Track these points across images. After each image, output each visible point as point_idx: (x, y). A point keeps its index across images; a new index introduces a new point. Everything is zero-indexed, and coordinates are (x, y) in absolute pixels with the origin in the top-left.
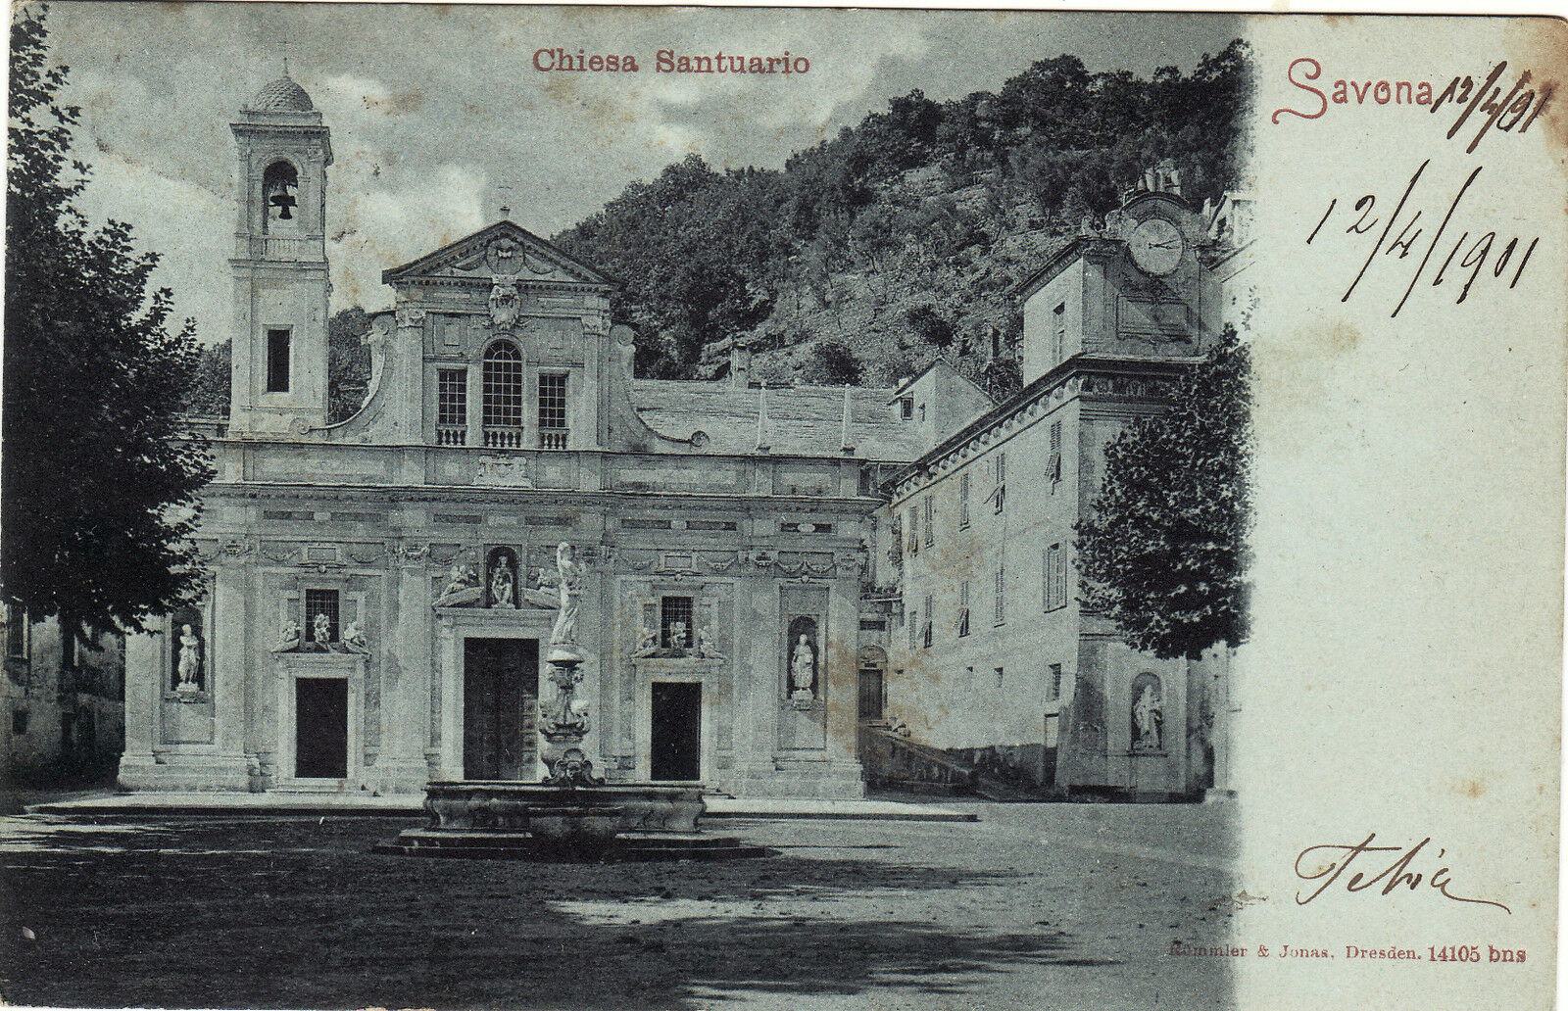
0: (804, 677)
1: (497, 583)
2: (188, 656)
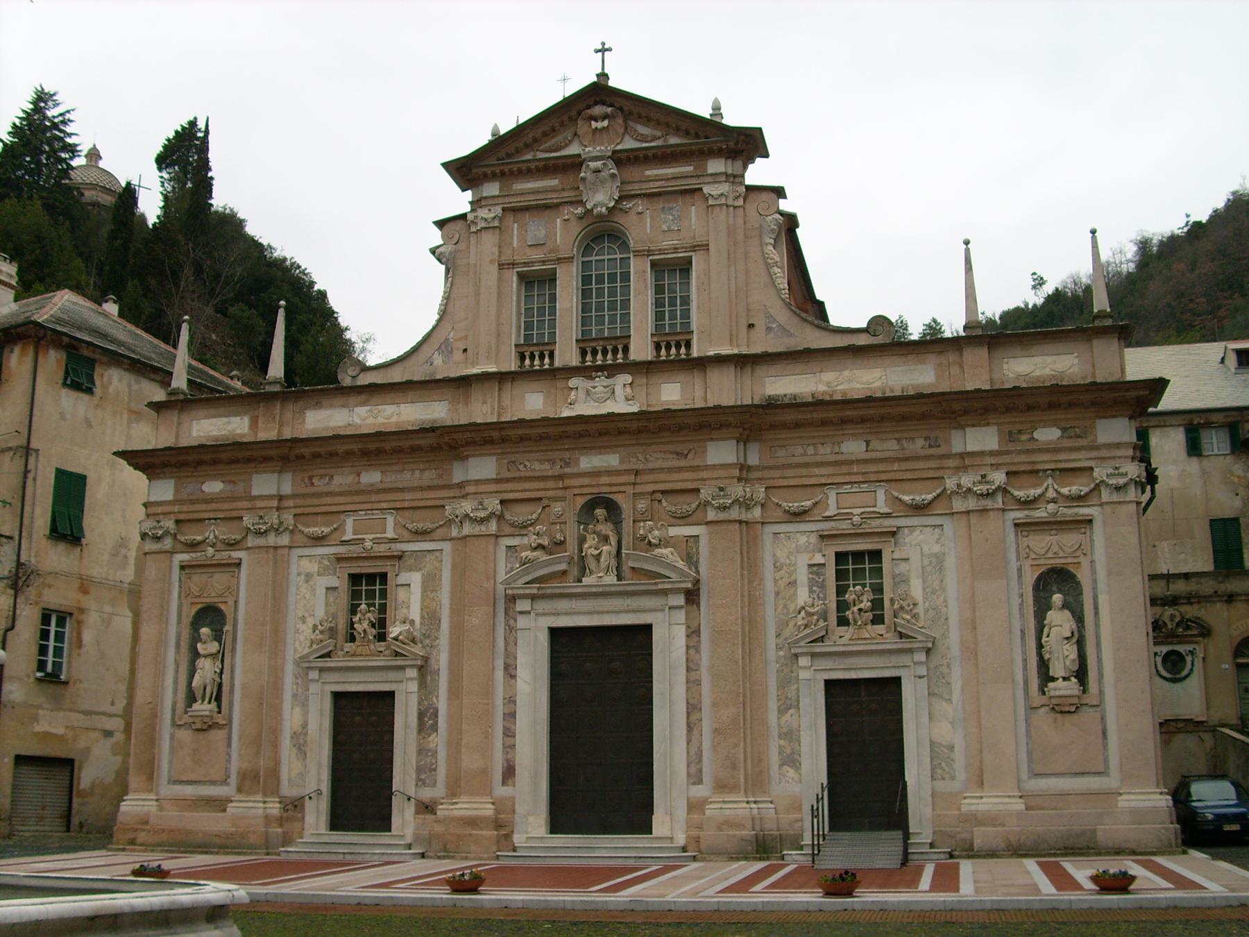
0: (1062, 658)
2: (206, 670)
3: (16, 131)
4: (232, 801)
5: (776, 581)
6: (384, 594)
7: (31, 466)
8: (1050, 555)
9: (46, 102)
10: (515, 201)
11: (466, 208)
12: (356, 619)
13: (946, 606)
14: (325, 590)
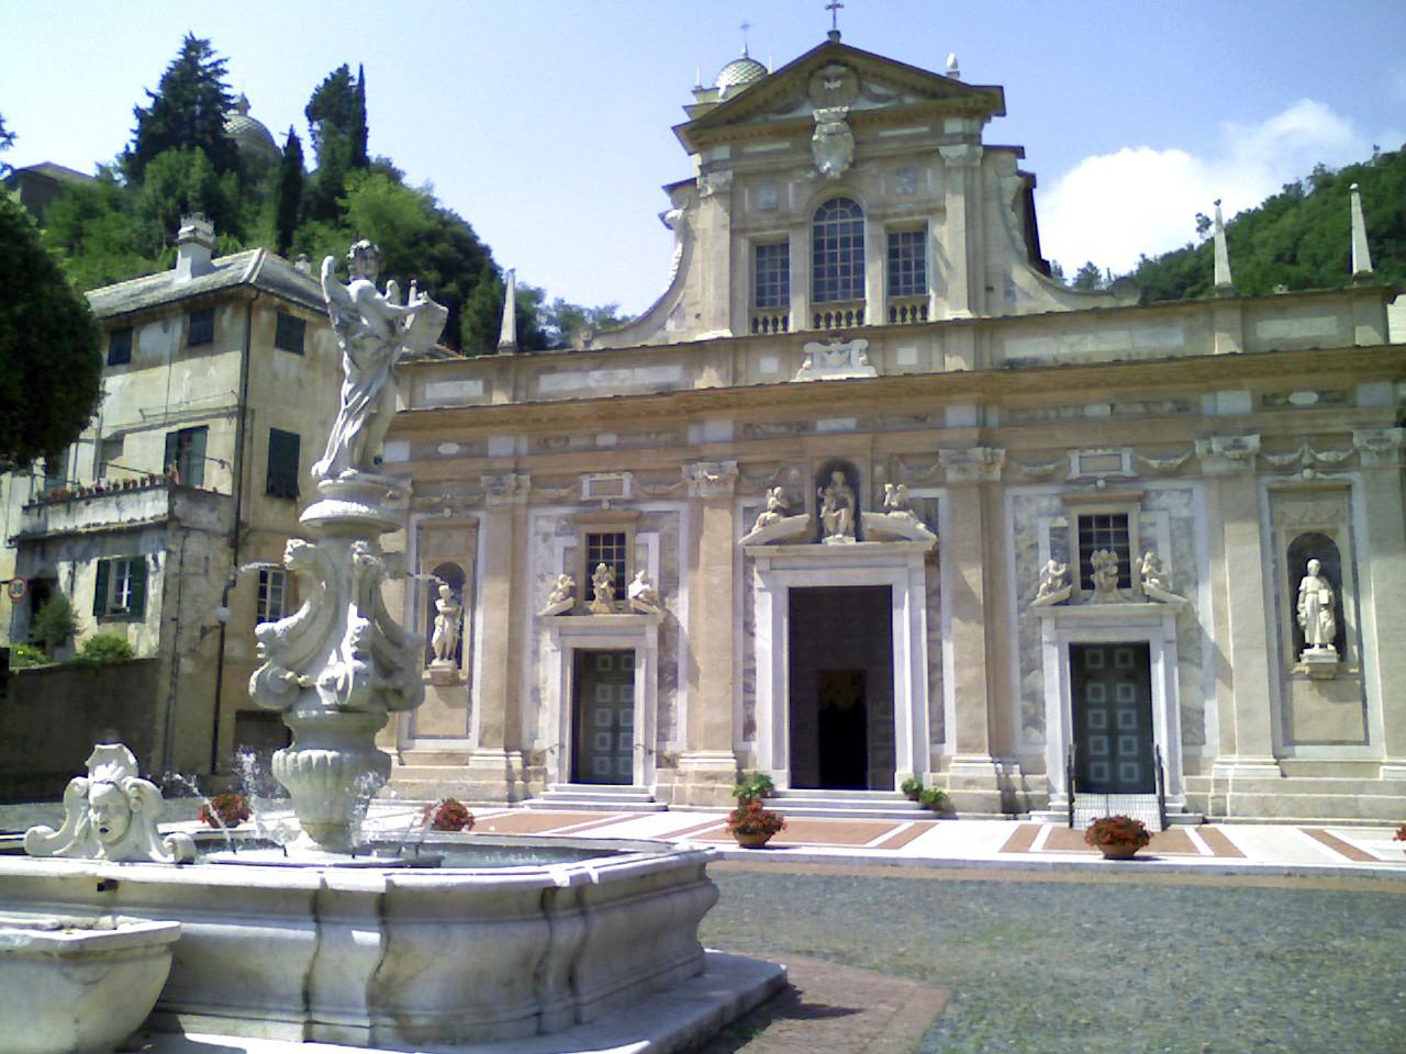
1: (828, 510)
3: (167, 81)
4: (472, 755)
5: (1016, 543)
6: (621, 553)
7: (248, 426)
8: (1306, 520)
9: (198, 52)
10: (745, 165)
11: (696, 173)
12: (594, 578)
13: (1196, 571)
14: (562, 550)
